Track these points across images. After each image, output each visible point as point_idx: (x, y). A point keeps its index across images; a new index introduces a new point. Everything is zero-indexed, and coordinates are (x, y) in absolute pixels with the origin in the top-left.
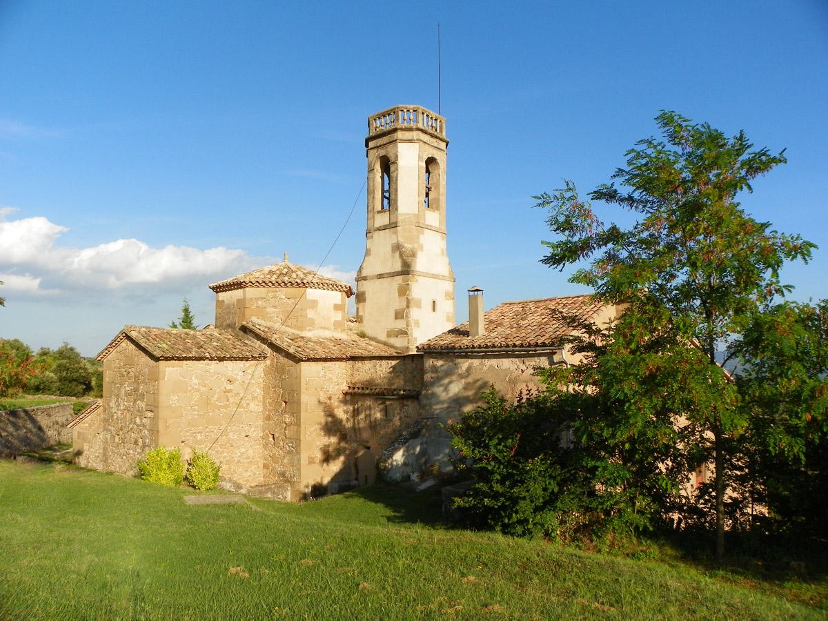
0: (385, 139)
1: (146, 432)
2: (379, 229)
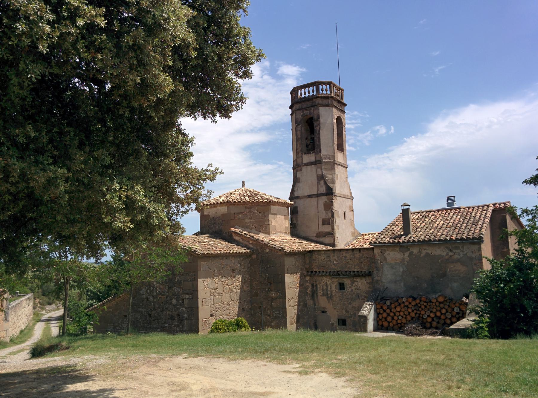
0: (309, 104)
1: (184, 309)
2: (307, 164)
